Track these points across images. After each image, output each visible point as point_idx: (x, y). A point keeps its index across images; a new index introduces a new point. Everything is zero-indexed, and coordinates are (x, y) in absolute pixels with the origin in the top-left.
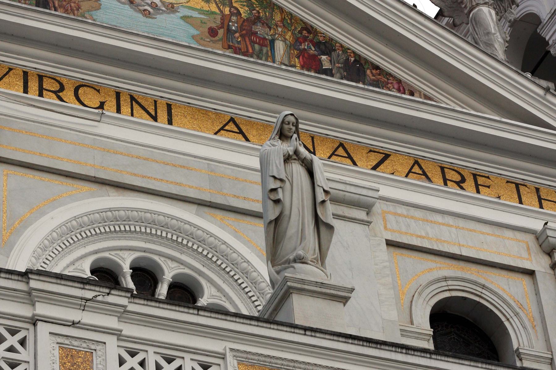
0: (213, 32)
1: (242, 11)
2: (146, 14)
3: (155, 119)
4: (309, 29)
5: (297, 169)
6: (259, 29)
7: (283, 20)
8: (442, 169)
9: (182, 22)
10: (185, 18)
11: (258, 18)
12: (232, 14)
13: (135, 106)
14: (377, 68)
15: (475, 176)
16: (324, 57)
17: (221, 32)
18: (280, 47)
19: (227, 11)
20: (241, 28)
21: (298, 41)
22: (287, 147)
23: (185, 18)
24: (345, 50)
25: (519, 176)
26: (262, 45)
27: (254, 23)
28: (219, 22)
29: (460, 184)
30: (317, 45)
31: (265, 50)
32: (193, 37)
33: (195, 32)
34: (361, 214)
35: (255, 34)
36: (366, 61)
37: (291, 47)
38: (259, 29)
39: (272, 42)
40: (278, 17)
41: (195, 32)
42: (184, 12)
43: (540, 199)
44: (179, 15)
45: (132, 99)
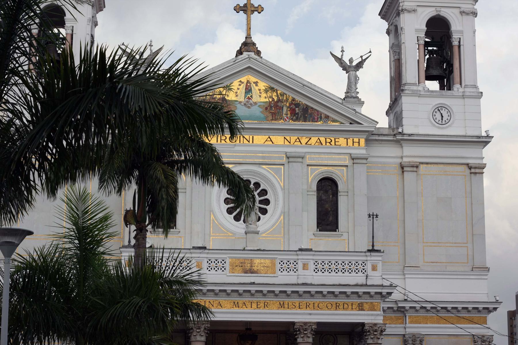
0: (266, 108)
1: (275, 99)
2: (249, 107)
3: (249, 142)
9: (258, 108)
10: (259, 106)
13: (244, 139)
14: (312, 108)
16: (297, 109)
17: (269, 108)
18: (285, 109)
19: (271, 100)
20: (274, 105)
21: (290, 105)
23: (259, 106)
26: (279, 109)
31: (280, 110)
32: (261, 112)
33: (261, 110)
34: (300, 160)
35: (278, 106)
36: (309, 106)
39: (283, 107)
40: (285, 98)
41: (261, 110)
42: (259, 104)
44: (258, 105)
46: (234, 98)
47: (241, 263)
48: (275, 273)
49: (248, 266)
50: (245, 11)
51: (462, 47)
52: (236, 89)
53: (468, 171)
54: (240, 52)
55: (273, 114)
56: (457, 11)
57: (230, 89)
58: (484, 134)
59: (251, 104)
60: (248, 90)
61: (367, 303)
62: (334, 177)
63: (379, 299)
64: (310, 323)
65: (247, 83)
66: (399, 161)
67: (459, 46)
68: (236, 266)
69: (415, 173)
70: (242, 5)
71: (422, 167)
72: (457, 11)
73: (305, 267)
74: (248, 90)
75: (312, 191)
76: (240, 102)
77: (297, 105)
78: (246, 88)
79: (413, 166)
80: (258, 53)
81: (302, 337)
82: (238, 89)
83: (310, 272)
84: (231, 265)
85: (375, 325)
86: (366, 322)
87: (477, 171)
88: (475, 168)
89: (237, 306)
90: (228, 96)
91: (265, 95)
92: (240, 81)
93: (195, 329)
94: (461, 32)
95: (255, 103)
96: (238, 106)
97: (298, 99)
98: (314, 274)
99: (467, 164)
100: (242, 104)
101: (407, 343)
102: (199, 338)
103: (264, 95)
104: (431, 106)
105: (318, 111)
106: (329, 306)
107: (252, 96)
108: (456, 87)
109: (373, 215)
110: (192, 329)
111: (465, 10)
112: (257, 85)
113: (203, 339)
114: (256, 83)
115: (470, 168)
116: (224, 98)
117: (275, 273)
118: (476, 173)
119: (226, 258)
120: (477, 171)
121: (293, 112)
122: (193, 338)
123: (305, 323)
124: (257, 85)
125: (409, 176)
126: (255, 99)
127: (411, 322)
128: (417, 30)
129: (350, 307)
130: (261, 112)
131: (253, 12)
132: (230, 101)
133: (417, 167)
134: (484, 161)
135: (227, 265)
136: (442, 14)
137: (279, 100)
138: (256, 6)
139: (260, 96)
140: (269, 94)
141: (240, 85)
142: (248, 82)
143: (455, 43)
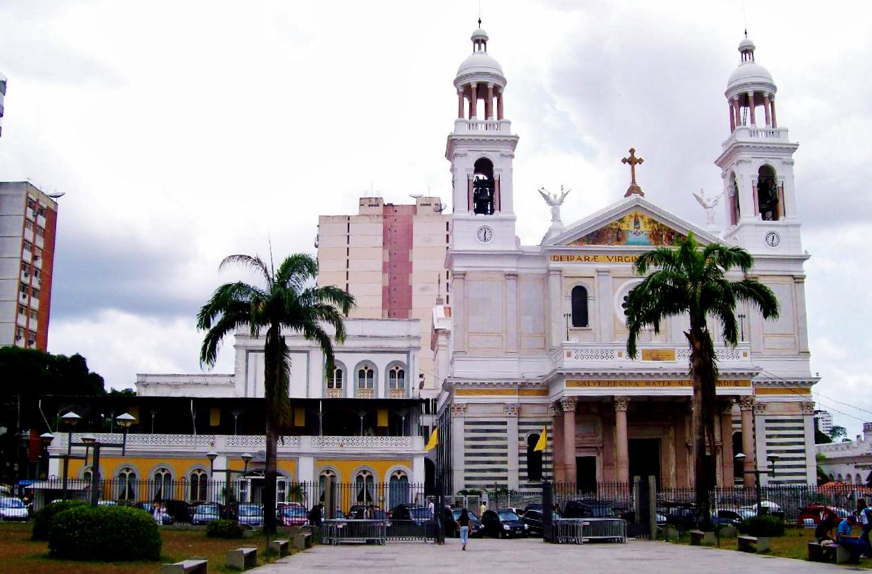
4: (670, 229)
6: (661, 233)
18: (664, 236)
33: (646, 237)
38: (661, 233)
46: (626, 229)
48: (674, 360)
49: (654, 355)
50: (630, 163)
51: (784, 189)
54: (628, 195)
55: (655, 239)
57: (624, 222)
58: (804, 253)
60: (637, 222)
67: (783, 188)
70: (628, 158)
72: (780, 161)
74: (637, 222)
77: (673, 233)
80: (642, 195)
84: (643, 353)
85: (748, 396)
86: (741, 394)
87: (800, 280)
92: (630, 216)
94: (784, 177)
96: (630, 234)
99: (792, 276)
102: (622, 409)
103: (648, 226)
104: (765, 233)
108: (781, 218)
111: (786, 161)
112: (643, 219)
113: (625, 409)
114: (642, 217)
115: (795, 279)
117: (674, 360)
118: (798, 282)
120: (800, 280)
121: (670, 239)
122: (617, 409)
124: (643, 219)
126: (642, 228)
128: (752, 176)
131: (636, 163)
134: (805, 274)
136: (770, 164)
137: (659, 230)
138: (638, 158)
140: (652, 225)
142: (636, 216)
143: (779, 185)
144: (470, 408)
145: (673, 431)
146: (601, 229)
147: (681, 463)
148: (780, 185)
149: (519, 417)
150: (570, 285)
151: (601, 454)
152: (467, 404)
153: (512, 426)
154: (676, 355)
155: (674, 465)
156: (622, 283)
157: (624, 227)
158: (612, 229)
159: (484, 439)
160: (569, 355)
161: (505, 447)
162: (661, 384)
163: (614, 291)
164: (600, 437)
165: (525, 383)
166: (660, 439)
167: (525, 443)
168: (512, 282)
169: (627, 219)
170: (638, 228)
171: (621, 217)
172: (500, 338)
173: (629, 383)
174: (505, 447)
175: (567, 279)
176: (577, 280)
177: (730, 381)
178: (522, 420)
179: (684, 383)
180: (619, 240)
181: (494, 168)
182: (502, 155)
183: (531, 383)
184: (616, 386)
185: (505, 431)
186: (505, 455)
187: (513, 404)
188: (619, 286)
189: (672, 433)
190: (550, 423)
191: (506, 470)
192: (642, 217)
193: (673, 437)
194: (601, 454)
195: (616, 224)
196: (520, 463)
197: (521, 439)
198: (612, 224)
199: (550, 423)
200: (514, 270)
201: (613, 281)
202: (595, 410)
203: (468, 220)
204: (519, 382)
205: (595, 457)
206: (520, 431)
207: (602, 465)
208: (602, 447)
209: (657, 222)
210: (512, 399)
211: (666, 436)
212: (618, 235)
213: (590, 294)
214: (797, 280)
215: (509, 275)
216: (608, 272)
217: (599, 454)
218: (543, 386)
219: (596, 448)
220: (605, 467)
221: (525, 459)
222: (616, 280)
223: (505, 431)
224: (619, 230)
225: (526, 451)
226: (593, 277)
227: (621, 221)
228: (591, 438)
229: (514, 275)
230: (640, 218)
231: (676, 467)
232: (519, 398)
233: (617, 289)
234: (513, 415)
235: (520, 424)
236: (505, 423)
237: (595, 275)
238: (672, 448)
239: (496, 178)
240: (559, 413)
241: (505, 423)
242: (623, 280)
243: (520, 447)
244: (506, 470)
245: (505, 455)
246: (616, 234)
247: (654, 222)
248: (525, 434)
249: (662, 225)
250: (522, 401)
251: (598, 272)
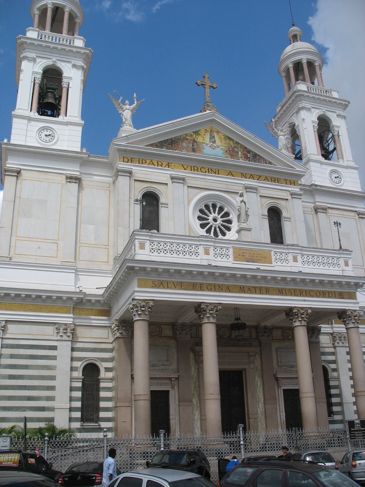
0: (226, 151)
2: (214, 149)
4: (245, 148)
5: (243, 203)
6: (236, 149)
7: (240, 146)
8: (271, 178)
9: (220, 150)
10: (221, 149)
11: (235, 147)
12: (230, 146)
13: (212, 171)
15: (278, 179)
17: (228, 151)
18: (240, 153)
20: (232, 150)
22: (241, 199)
23: (221, 149)
24: (253, 152)
25: (286, 178)
27: (235, 148)
28: (228, 149)
29: (274, 181)
30: (247, 151)
31: (237, 154)
32: (223, 153)
33: (223, 152)
37: (242, 153)
38: (236, 149)
39: (238, 152)
40: (239, 146)
41: (223, 152)
42: (221, 147)
43: (290, 183)
44: (220, 148)
45: (211, 169)
46: (201, 141)
47: (243, 253)
52: (203, 134)
53: (357, 217)
56: (335, 115)
57: (199, 134)
59: (215, 147)
60: (212, 137)
61: (345, 292)
62: (279, 206)
63: (354, 290)
64: (306, 308)
65: (211, 131)
66: (313, 205)
67: (338, 136)
68: (240, 255)
69: (325, 214)
71: (327, 209)
73: (295, 260)
75: (265, 216)
76: (207, 144)
77: (249, 151)
78: (210, 135)
79: (323, 209)
81: (300, 321)
82: (205, 135)
83: (299, 264)
84: (234, 253)
85: (355, 311)
88: (362, 214)
89: (243, 291)
90: (197, 139)
91: (224, 142)
93: (208, 311)
95: (218, 147)
96: (206, 147)
97: (249, 147)
98: (302, 265)
100: (208, 145)
101: (335, 339)
102: (212, 320)
104: (329, 171)
105: (263, 158)
106: (318, 294)
107: (215, 141)
109: (337, 223)
110: (205, 311)
112: (218, 134)
116: (195, 140)
118: (362, 218)
119: (230, 247)
123: (302, 308)
125: (321, 215)
126: (218, 142)
127: (335, 324)
128: (313, 122)
129: (334, 295)
130: (223, 153)
132: (199, 142)
133: (326, 209)
135: (231, 253)
139: (221, 142)
140: (228, 141)
141: (205, 132)
144: (11, 328)
145: (259, 360)
146: (175, 138)
147: (269, 399)
148: (337, 134)
149: (72, 341)
150: (139, 190)
151: (176, 388)
152: (6, 321)
153: (64, 348)
154: (273, 258)
155: (262, 400)
156: (197, 194)
157: (199, 139)
158: (187, 139)
159: (26, 367)
160: (142, 247)
161: (53, 378)
162: (258, 290)
163: (189, 203)
164: (174, 366)
165: (82, 299)
166: (245, 369)
167: (78, 374)
168: (74, 186)
169: (202, 132)
170: (214, 142)
171: (197, 129)
172: (56, 244)
173: (220, 288)
174: (53, 378)
175: (136, 182)
176: (148, 185)
177: (335, 292)
178: (78, 345)
179: (284, 291)
180: (194, 150)
181: (65, 75)
182: (74, 66)
183: (90, 300)
184: (203, 290)
185: (54, 358)
186: (52, 388)
187: (66, 324)
188: (194, 196)
189: (258, 363)
190: (111, 350)
191: (52, 409)
192: (218, 132)
193: (259, 368)
194: (176, 388)
195: (191, 136)
196: (71, 399)
197: (72, 369)
198: (186, 135)
199: (111, 350)
200: (78, 174)
201: (188, 193)
202: (168, 332)
203: (29, 119)
204: (75, 297)
205: (168, 391)
206: (72, 359)
207: (177, 403)
208: (177, 379)
209: (233, 140)
210: (67, 319)
211: (252, 366)
212: (193, 146)
213: (162, 200)
214: (360, 216)
215: (71, 178)
216: (183, 179)
217: (173, 387)
218: (104, 304)
219: (170, 379)
220: (181, 404)
221: (79, 394)
222: (191, 190)
223: (54, 358)
224: (194, 141)
225: (80, 385)
226: (167, 184)
227: (197, 133)
228: (163, 367)
229: (76, 178)
230: (215, 134)
231: (265, 404)
232: (74, 318)
233: (192, 199)
234: (67, 338)
235: (73, 349)
236: (54, 348)
237: (169, 182)
238: (259, 382)
239: (64, 85)
240: (124, 334)
241: (54, 348)
242: (198, 191)
243: (72, 379)
244: (52, 409)
245: (52, 388)
246: (191, 145)
247: (230, 139)
248: (81, 362)
249: (237, 143)
250: (78, 322)
251: (172, 178)
